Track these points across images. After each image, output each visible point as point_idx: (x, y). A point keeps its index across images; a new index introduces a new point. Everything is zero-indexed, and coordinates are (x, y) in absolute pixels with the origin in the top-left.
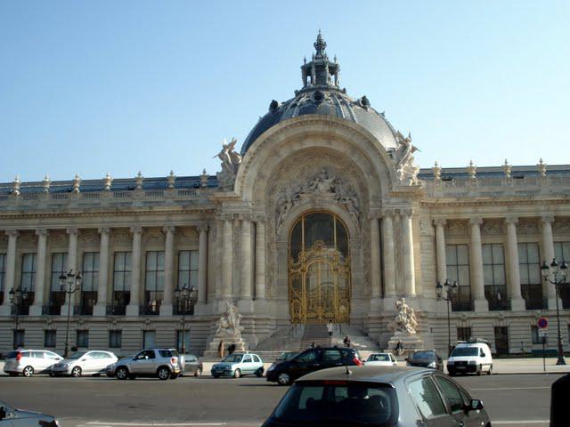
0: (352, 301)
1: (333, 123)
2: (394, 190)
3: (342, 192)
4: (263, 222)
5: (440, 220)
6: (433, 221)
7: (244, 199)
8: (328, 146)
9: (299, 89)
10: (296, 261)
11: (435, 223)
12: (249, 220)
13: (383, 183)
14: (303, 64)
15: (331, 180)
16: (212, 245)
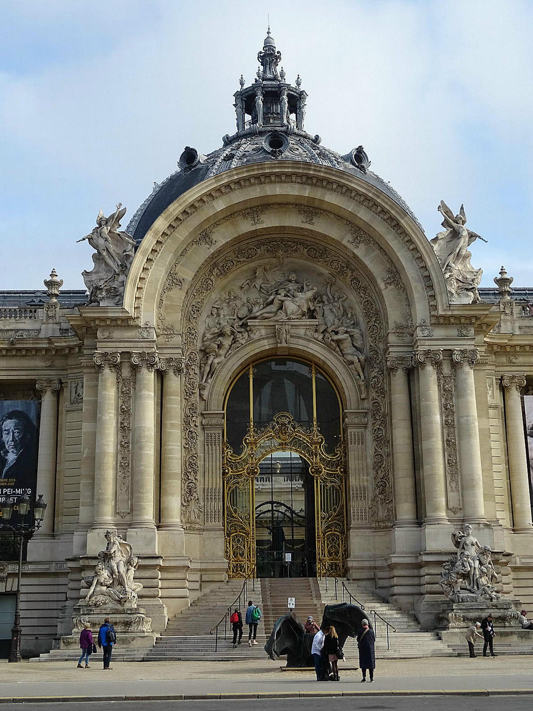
0: (352, 533)
1: (322, 179)
2: (441, 312)
3: (330, 317)
4: (178, 371)
5: (513, 377)
6: (501, 379)
7: (142, 324)
8: (307, 226)
9: (233, 131)
10: (238, 451)
11: (506, 382)
12: (151, 366)
13: (416, 295)
14: (238, 88)
15: (310, 294)
16: (67, 419)
